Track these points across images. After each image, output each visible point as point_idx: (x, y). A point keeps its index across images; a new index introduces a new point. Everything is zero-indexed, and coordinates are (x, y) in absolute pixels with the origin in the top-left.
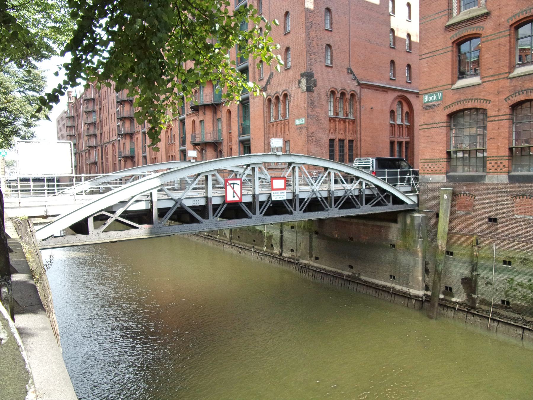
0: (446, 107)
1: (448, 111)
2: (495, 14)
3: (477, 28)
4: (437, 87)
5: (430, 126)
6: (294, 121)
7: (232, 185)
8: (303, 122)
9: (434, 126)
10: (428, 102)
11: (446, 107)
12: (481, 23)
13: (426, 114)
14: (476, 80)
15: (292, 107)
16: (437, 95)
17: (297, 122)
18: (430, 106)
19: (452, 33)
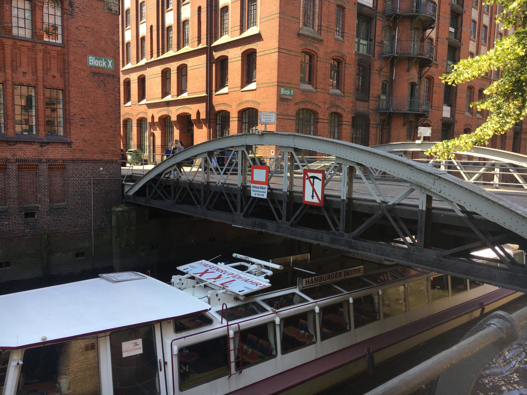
0: (296, 104)
1: (296, 108)
2: (325, 43)
3: (316, 47)
4: (290, 83)
5: (285, 117)
6: (85, 57)
7: (312, 180)
8: (110, 65)
9: (288, 117)
10: (284, 95)
11: (296, 104)
12: (318, 46)
13: (282, 105)
14: (309, 87)
15: (77, 28)
16: (290, 90)
17: (92, 61)
18: (285, 99)
19: (302, 42)
